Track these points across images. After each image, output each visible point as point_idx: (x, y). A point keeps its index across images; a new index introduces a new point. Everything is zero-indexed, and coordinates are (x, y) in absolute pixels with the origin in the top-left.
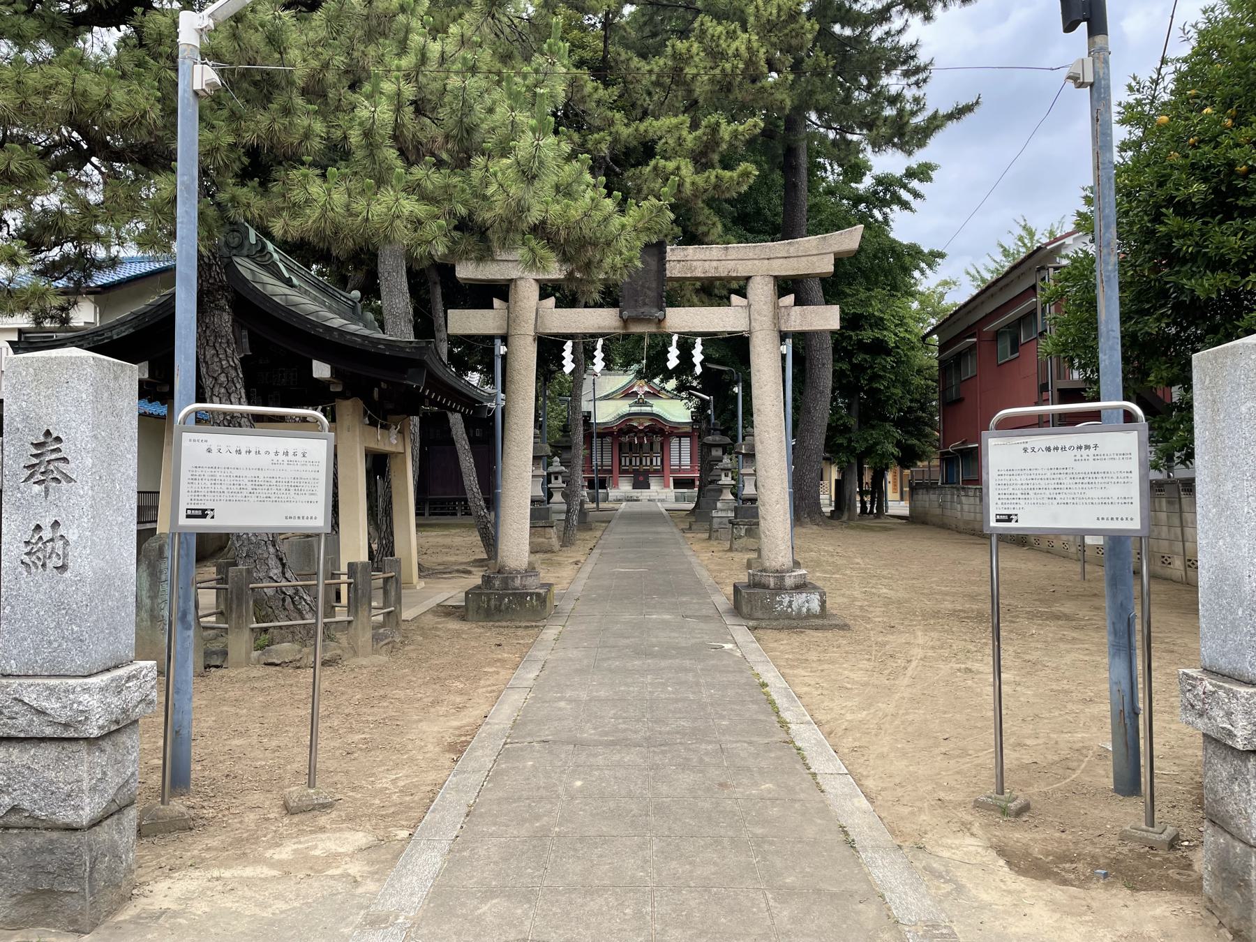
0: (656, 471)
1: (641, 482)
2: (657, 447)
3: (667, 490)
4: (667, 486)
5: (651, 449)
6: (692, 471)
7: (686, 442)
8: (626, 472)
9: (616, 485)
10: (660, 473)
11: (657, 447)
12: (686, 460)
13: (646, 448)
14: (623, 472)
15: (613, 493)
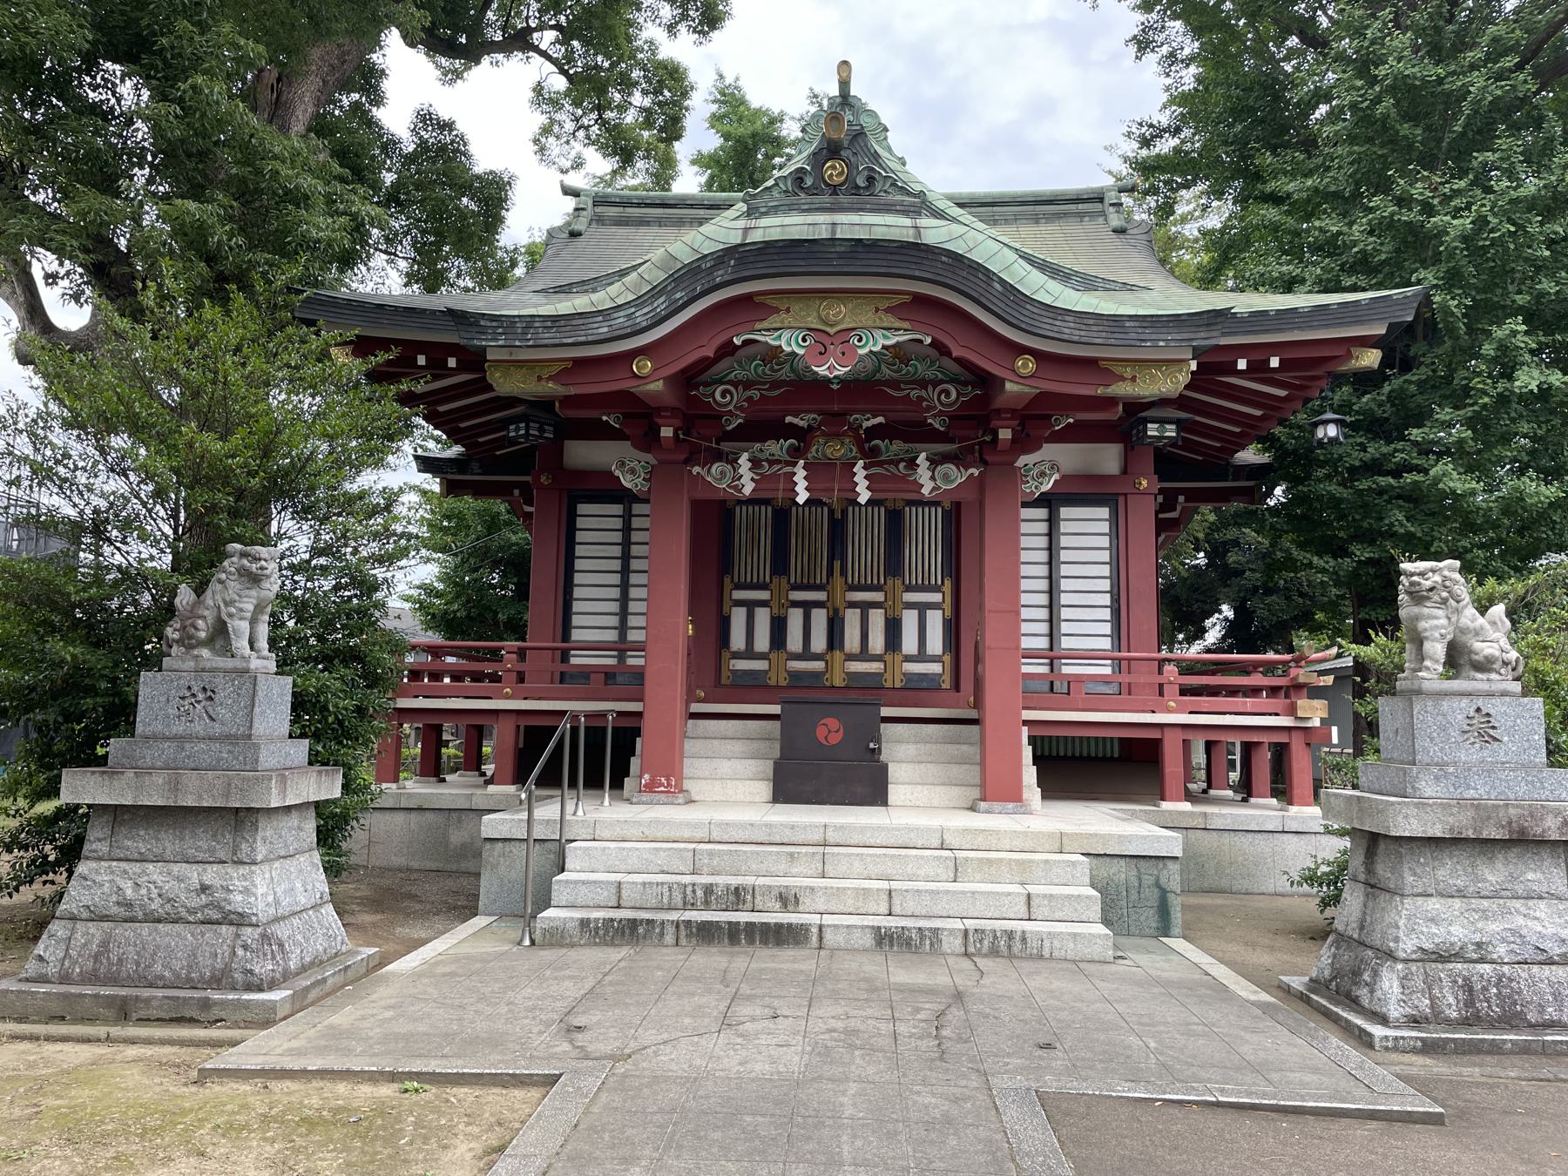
0: (918, 689)
1: (828, 762)
2: (925, 544)
3: (996, 821)
4: (994, 789)
5: (894, 564)
6: (1125, 693)
7: (1087, 530)
8: (751, 687)
9: (669, 781)
10: (957, 694)
11: (925, 544)
12: (1088, 627)
13: (865, 548)
14: (717, 682)
15: (613, 843)
